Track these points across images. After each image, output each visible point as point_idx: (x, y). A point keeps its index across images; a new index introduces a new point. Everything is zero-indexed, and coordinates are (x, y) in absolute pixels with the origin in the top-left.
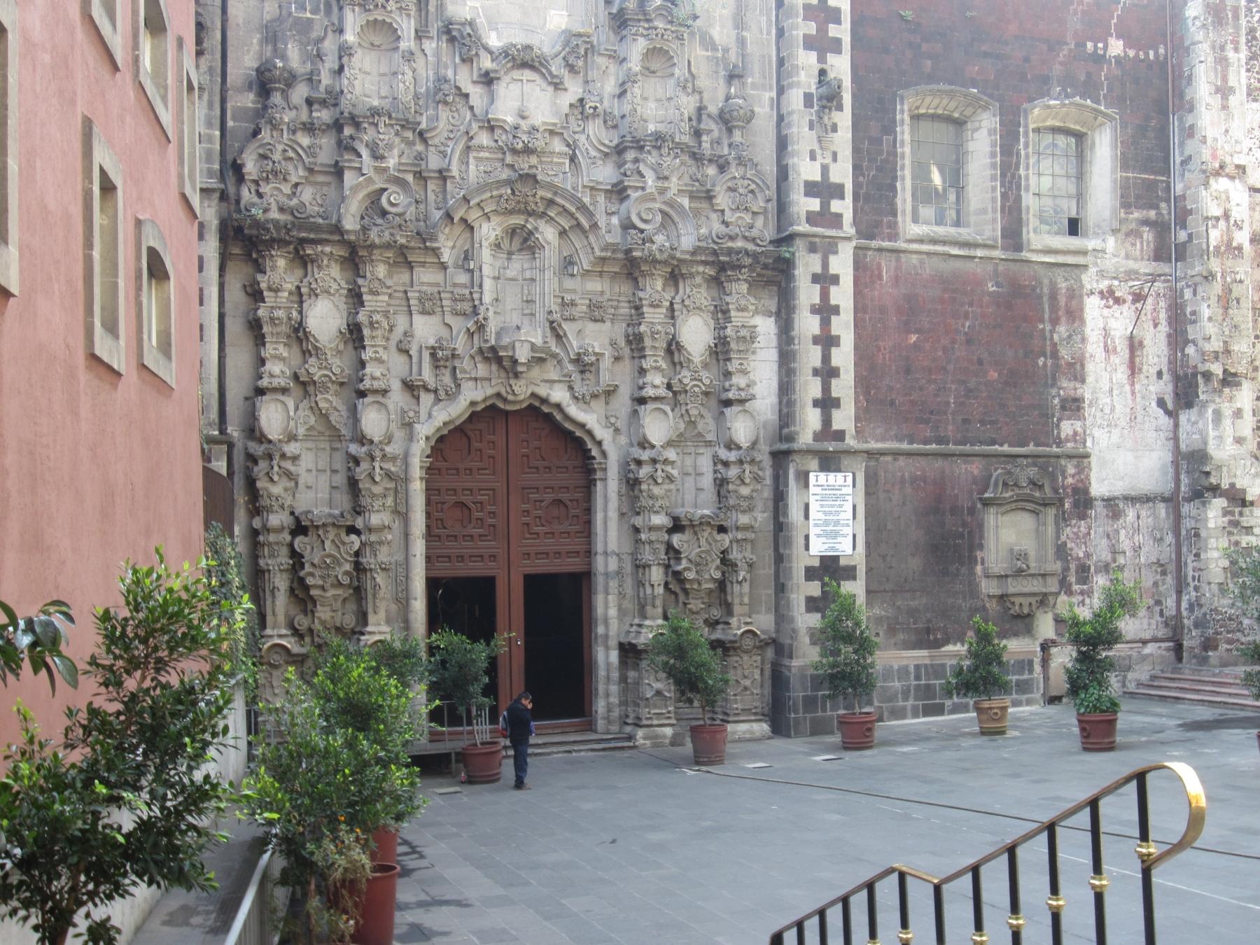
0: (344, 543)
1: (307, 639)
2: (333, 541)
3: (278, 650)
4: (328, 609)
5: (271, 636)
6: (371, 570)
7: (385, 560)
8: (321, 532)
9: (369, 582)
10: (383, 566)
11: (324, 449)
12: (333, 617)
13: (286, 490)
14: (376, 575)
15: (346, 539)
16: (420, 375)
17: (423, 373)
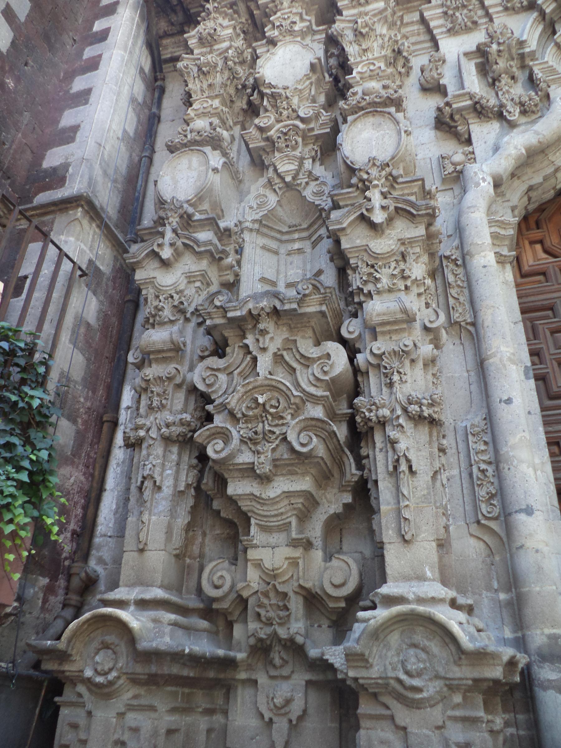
0: (306, 361)
1: (238, 631)
2: (278, 358)
3: (111, 639)
4: (279, 538)
5: (121, 604)
6: (382, 423)
7: (417, 394)
8: (250, 340)
9: (380, 457)
10: (413, 408)
11: (300, 251)
12: (294, 563)
13: (190, 279)
14: (392, 433)
15: (313, 352)
16: (463, 88)
17: (466, 84)
